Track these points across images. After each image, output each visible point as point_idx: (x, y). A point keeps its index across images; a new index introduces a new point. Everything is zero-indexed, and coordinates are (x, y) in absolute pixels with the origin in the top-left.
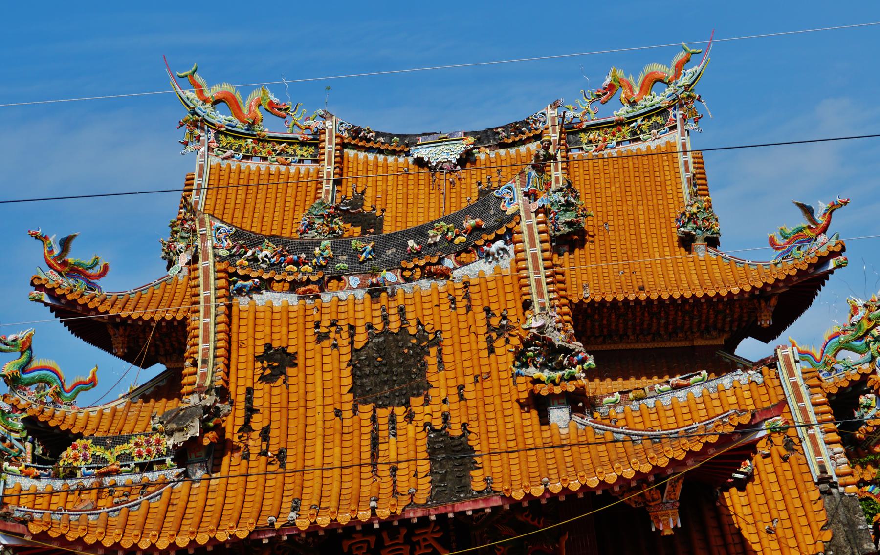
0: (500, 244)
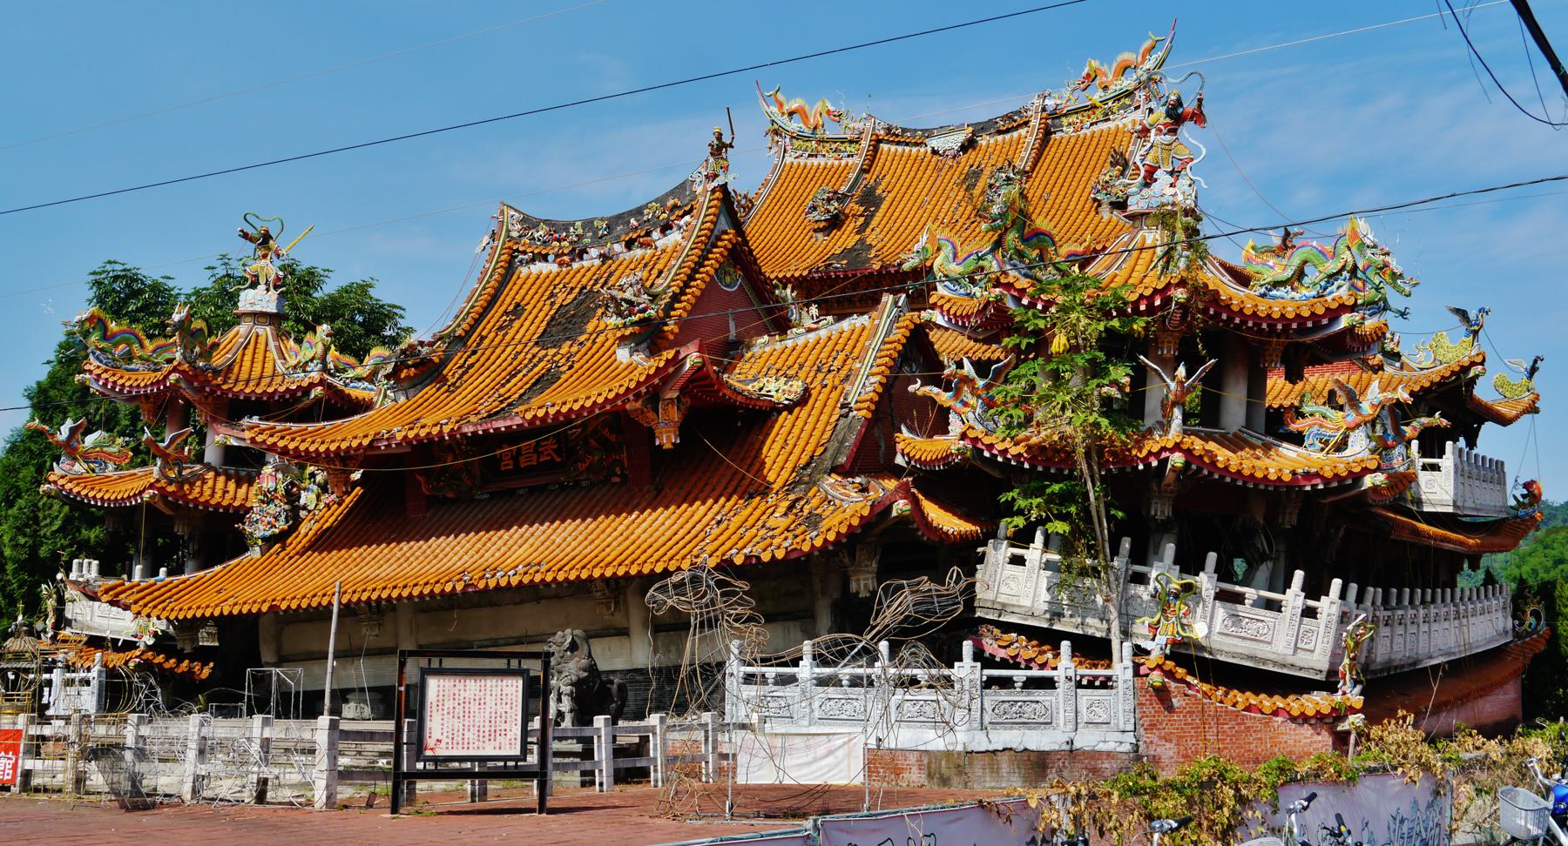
0: (687, 218)
